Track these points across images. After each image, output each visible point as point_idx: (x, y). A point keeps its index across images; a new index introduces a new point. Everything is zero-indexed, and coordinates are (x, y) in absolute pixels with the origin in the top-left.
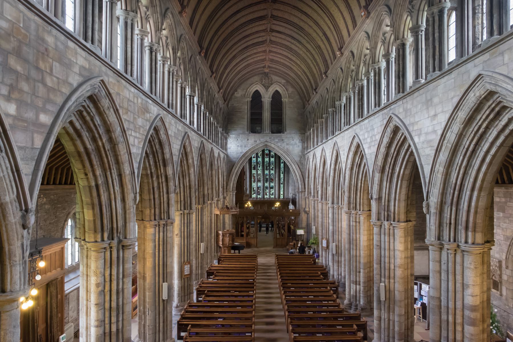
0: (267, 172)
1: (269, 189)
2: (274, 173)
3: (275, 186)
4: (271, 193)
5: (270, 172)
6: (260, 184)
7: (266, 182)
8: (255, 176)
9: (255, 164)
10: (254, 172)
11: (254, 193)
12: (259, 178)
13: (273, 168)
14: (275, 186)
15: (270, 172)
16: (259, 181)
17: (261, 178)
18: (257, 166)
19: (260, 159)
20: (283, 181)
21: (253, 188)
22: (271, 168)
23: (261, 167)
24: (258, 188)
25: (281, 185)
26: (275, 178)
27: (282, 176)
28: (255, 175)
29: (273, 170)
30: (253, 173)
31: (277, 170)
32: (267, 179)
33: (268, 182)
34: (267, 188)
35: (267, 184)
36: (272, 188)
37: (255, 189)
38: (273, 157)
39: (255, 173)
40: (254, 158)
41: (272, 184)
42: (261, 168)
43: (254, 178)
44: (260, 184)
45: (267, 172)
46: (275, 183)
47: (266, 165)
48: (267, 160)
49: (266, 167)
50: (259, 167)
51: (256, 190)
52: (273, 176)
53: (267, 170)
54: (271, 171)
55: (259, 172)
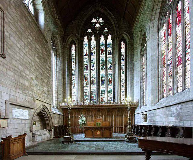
1: (106, 93)
2: (112, 73)
3: (114, 88)
4: (109, 98)
5: (107, 72)
6: (94, 88)
7: (103, 83)
8: (87, 78)
9: (88, 63)
10: (86, 72)
11: (86, 99)
13: (111, 66)
14: (114, 88)
15: (107, 72)
16: (93, 83)
17: (95, 80)
19: (94, 57)
20: (124, 82)
22: (108, 67)
23: (95, 66)
24: (91, 92)
25: (122, 88)
26: (114, 78)
27: (123, 76)
28: (88, 77)
29: (111, 69)
30: (84, 74)
31: (117, 68)
32: (103, 81)
33: (105, 85)
34: (103, 92)
35: (103, 88)
37: (87, 94)
38: (110, 54)
39: (88, 74)
41: (110, 87)
42: (95, 67)
43: (86, 80)
44: (94, 88)
45: (103, 72)
46: (114, 85)
48: (102, 57)
49: (102, 65)
50: (93, 66)
51: (89, 95)
53: (102, 69)
54: (108, 70)
55: (94, 73)
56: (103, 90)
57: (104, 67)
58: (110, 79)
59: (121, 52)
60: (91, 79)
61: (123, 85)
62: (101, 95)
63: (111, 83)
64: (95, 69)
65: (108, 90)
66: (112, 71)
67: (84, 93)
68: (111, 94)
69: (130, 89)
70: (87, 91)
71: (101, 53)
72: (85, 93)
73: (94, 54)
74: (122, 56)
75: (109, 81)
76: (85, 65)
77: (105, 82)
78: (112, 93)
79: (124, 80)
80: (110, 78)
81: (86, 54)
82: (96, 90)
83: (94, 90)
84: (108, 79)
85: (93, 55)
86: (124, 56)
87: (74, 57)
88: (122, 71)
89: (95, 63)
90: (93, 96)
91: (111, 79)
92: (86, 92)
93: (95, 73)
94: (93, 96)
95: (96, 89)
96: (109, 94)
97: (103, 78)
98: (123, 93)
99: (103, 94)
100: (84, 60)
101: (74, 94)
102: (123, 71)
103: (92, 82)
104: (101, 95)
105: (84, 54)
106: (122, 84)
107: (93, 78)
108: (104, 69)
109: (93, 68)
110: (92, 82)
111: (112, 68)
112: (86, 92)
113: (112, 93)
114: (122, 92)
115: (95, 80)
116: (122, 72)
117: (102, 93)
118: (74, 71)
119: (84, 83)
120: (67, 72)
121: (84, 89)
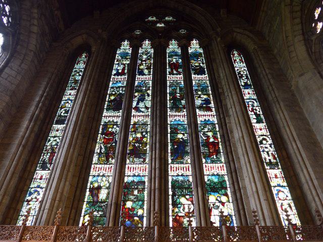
0: (178, 118)
5: (192, 117)
8: (112, 134)
12: (137, 140)
14: (234, 172)
15: (192, 117)
16: (137, 153)
18: (131, 97)
19: (146, 78)
21: (95, 191)
22: (198, 102)
25: (271, 172)
27: (261, 130)
29: (209, 109)
33: (188, 159)
34: (180, 187)
35: (180, 171)
36: (218, 188)
37: (103, 195)
40: (118, 74)
41: (214, 170)
45: (178, 118)
47: (173, 94)
50: (142, 99)
52: (213, 130)
53: (176, 107)
55: (142, 116)
56: (181, 178)
57: (183, 102)
58: (212, 140)
59: (236, 69)
60: (131, 139)
61: (272, 160)
62: (175, 204)
63: (217, 152)
64: (147, 108)
65: (206, 178)
66: (214, 113)
67: (88, 193)
68: (224, 199)
69: (315, 172)
70: (104, 183)
71: (168, 70)
72: (91, 190)
73: (146, 72)
74: (241, 77)
75: (207, 144)
76: (112, 98)
77: (188, 149)
78: (226, 195)
79: (270, 142)
80: (210, 134)
81: (120, 71)
82: (146, 179)
83: (136, 179)
84: (202, 138)
85: (144, 74)
86: (247, 78)
87: (79, 78)
88: (253, 117)
89: (150, 92)
90: (129, 204)
91: (215, 137)
92: (99, 188)
93: (148, 120)
94: (129, 204)
95: (147, 173)
96: (212, 198)
97: (180, 136)
98: (281, 195)
99: (183, 200)
100: (111, 85)
101: (34, 196)
102: (257, 116)
103: (130, 148)
104: (175, 204)
105: (114, 72)
106: (264, 155)
107: (139, 135)
108: (184, 107)
109: (141, 105)
110: (130, 148)
111: (212, 105)
112: (99, 188)
113: (226, 195)
114: (275, 192)
115: (147, 139)
116: (254, 117)
117: (178, 192)
118: (67, 112)
119: (97, 150)
120: (33, 108)
121: (92, 172)
